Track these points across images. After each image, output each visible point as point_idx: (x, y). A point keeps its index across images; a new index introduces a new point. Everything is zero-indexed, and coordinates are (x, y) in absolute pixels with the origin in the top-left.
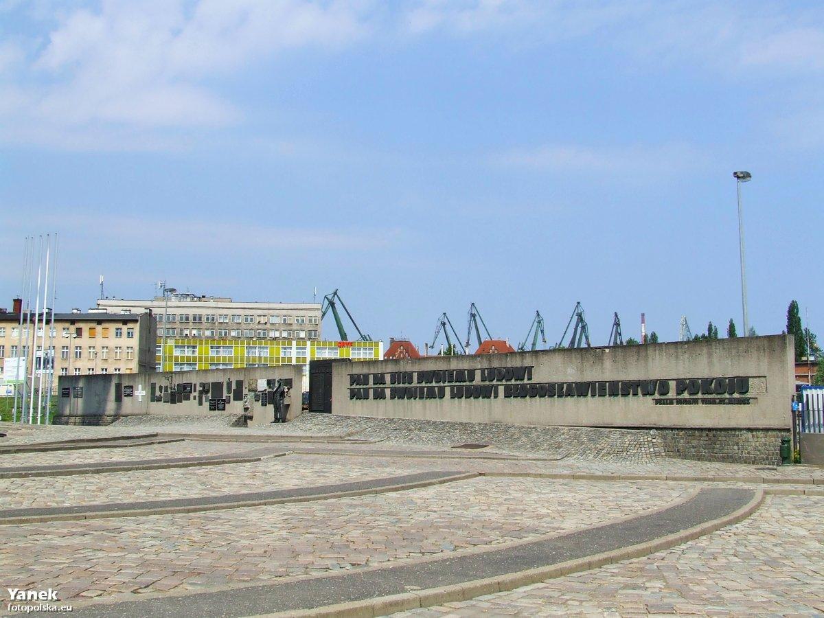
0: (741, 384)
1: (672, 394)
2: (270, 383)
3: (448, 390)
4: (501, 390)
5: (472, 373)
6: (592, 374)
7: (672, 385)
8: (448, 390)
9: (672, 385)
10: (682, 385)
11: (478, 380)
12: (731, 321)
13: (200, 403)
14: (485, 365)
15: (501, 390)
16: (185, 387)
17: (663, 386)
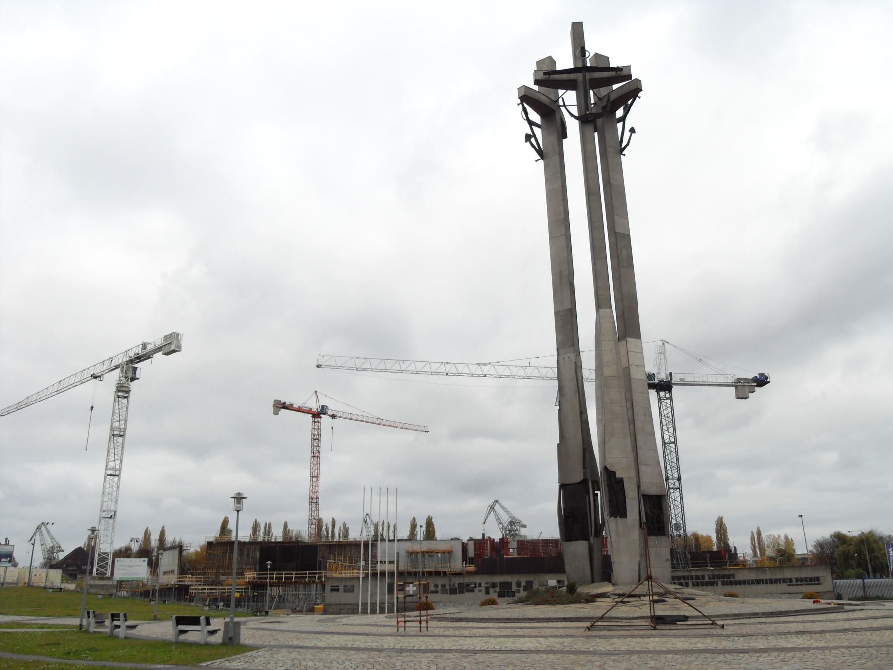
0: (818, 579)
1: (794, 582)
2: (558, 582)
3: (690, 584)
4: (720, 583)
5: (703, 577)
6: (762, 576)
7: (794, 580)
8: (690, 584)
9: (794, 580)
10: (797, 580)
11: (707, 579)
12: (163, 527)
13: (487, 592)
14: (710, 573)
15: (720, 583)
16: (468, 585)
17: (791, 580)
